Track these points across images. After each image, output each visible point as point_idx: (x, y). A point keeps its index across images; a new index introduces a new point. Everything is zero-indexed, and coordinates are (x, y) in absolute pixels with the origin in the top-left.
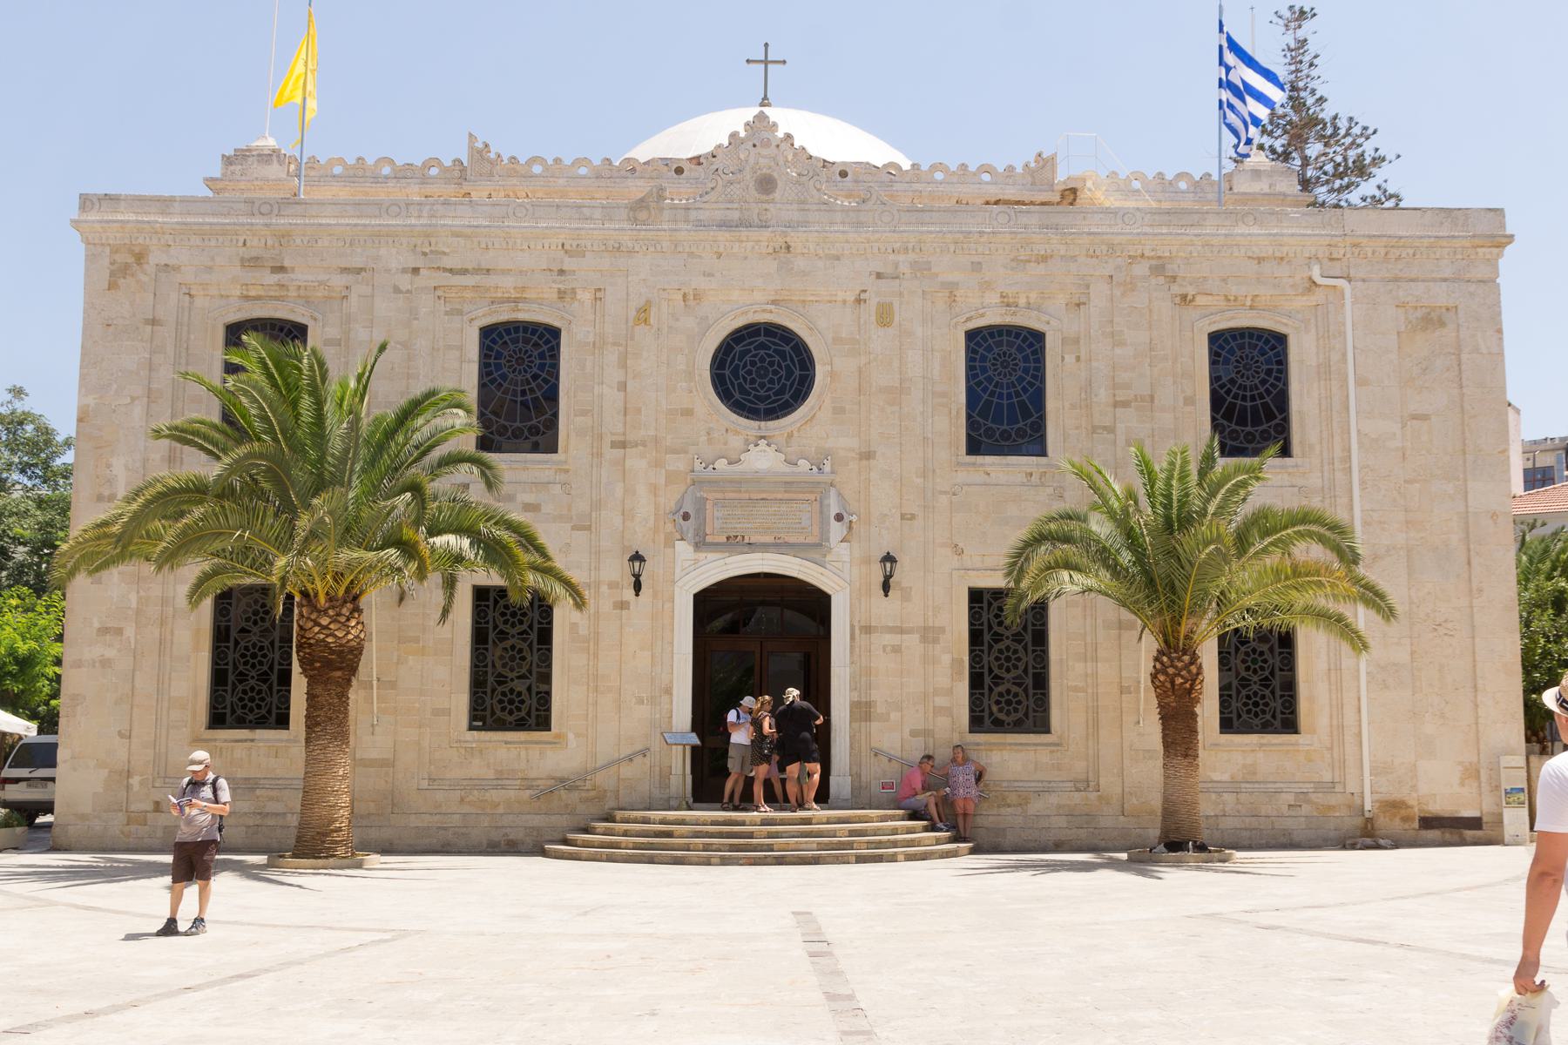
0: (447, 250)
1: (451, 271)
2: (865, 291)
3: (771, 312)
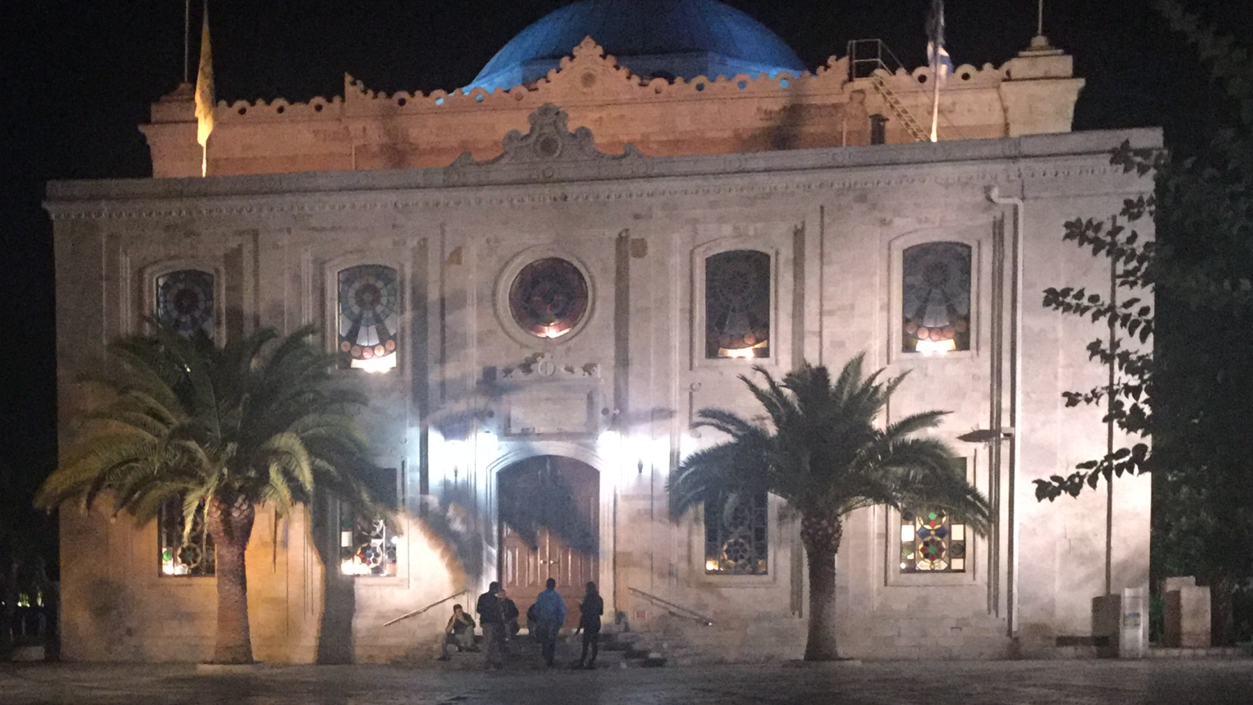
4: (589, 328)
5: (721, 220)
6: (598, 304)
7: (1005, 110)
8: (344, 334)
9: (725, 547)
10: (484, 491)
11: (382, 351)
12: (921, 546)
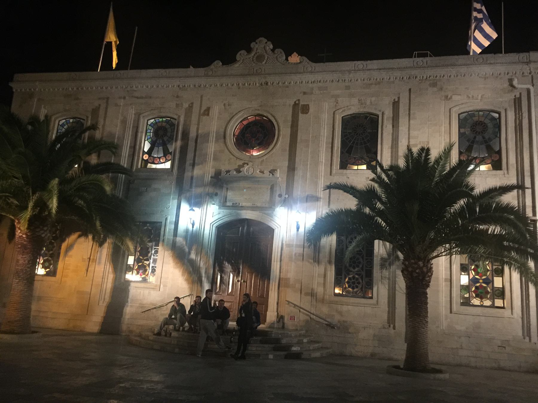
1: (137, 98)
3: (259, 110)
4: (274, 150)
5: (351, 96)
6: (281, 138)
9: (347, 280)
10: (207, 238)
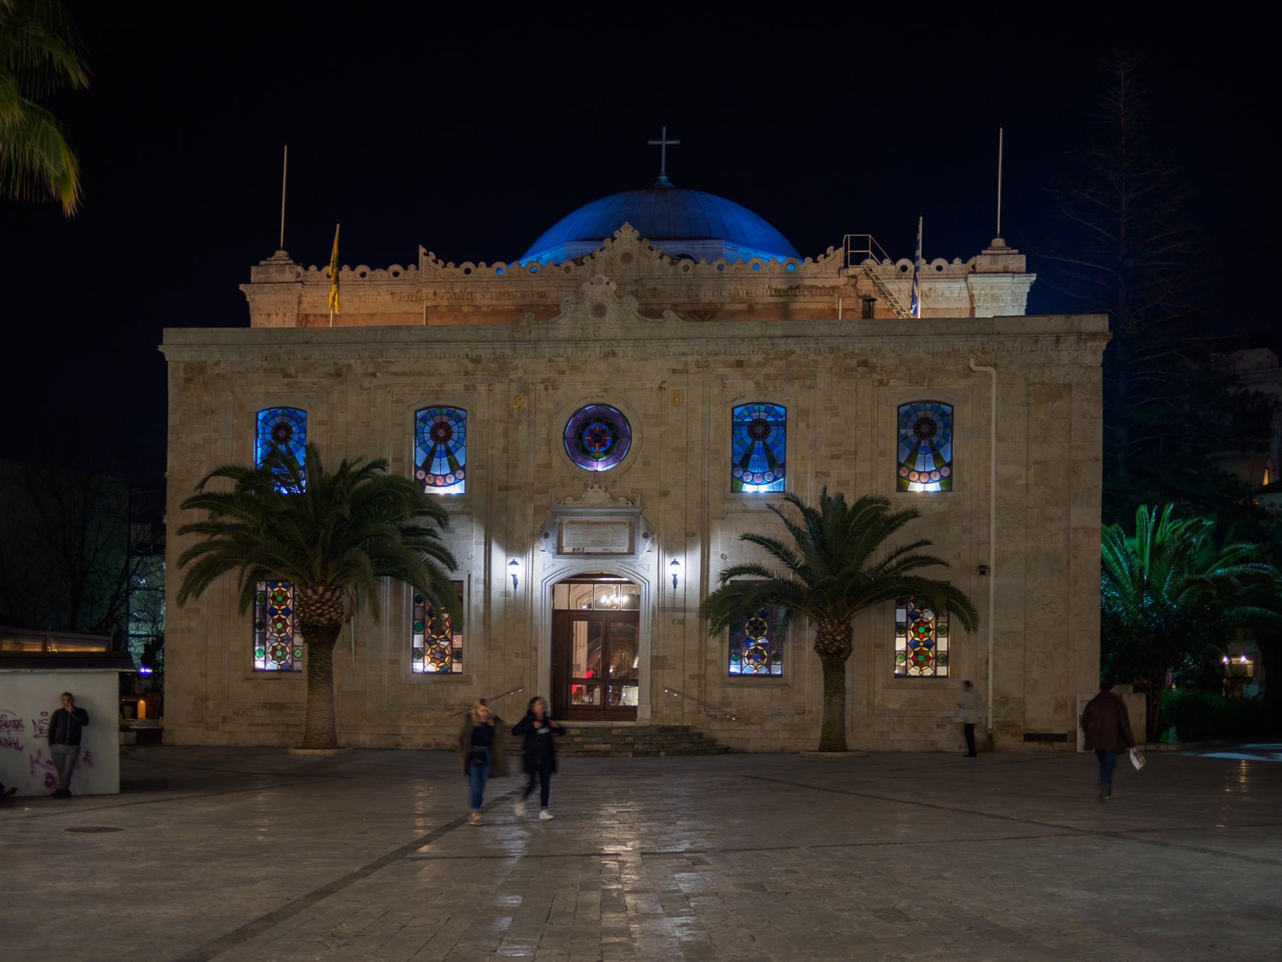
0: (393, 360)
1: (396, 374)
2: (664, 382)
7: (971, 297)
8: (420, 465)
11: (453, 480)
12: (911, 656)
